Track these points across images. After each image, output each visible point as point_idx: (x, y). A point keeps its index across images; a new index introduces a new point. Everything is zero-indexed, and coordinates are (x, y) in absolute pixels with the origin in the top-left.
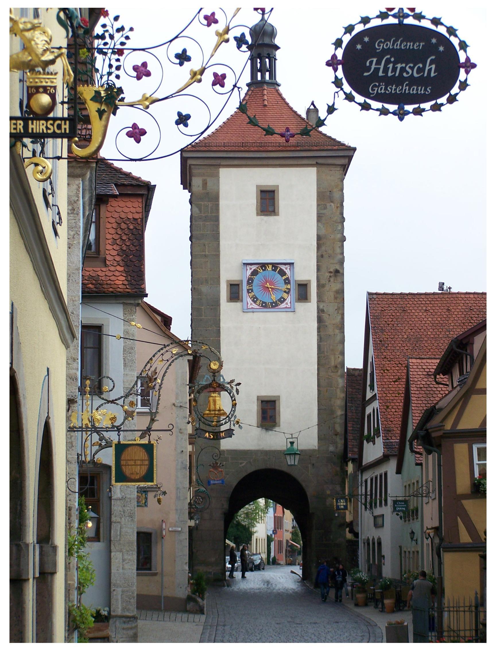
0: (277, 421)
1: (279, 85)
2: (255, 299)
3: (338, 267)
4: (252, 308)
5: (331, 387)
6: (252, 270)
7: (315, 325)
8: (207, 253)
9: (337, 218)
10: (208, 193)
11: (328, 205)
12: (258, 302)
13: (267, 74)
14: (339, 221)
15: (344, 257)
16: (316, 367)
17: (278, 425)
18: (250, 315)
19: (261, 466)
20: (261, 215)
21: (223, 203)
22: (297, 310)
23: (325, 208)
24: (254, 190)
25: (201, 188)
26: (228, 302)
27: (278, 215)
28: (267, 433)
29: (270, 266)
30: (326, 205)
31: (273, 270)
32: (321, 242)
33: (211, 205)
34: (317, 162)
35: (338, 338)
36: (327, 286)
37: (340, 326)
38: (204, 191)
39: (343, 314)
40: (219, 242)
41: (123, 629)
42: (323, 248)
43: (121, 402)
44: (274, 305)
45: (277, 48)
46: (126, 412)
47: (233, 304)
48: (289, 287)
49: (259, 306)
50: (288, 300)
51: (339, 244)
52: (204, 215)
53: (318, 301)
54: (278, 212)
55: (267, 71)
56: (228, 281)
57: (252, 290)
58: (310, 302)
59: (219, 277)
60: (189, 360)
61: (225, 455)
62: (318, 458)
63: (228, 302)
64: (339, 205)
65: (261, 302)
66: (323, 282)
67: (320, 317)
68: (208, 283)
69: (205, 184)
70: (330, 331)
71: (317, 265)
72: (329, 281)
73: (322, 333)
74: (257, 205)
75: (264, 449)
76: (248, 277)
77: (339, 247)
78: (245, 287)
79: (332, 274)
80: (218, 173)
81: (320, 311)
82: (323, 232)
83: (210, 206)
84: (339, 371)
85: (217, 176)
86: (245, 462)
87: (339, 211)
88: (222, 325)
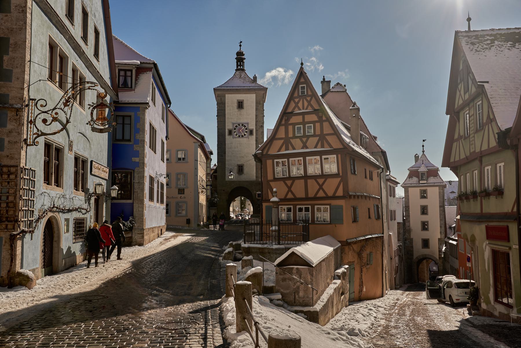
1: (245, 70)
3: (262, 125)
7: (255, 142)
9: (262, 109)
11: (259, 106)
13: (242, 67)
18: (235, 139)
23: (258, 107)
41: (138, 234)
43: (50, 112)
44: (242, 136)
45: (245, 59)
46: (53, 118)
55: (242, 66)
56: (228, 129)
60: (199, 145)
66: (257, 129)
69: (221, 99)
81: (256, 138)
85: (225, 97)
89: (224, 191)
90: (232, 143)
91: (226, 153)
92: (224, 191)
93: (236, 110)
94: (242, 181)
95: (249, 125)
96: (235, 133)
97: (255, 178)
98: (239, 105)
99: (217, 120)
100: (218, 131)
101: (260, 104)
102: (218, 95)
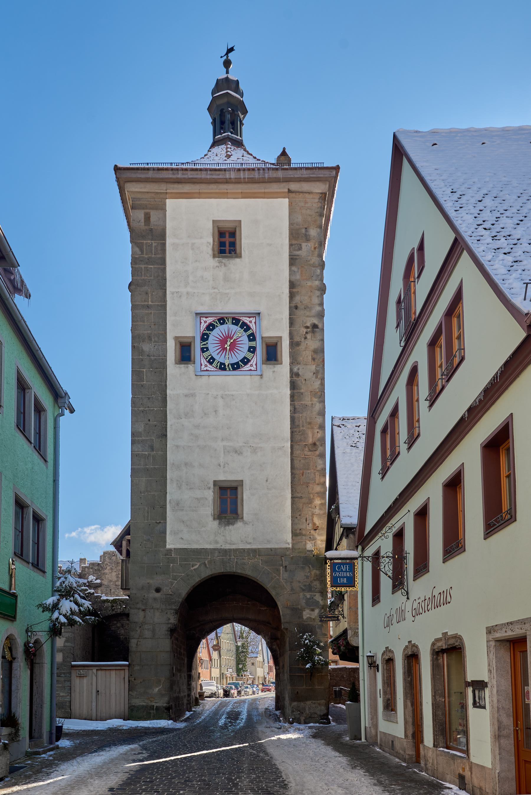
0: (239, 512)
2: (211, 360)
3: (316, 321)
4: (207, 370)
5: (308, 469)
6: (207, 324)
7: (288, 392)
8: (150, 303)
10: (151, 230)
11: (304, 245)
12: (214, 364)
14: (317, 263)
15: (323, 310)
16: (289, 444)
17: (240, 517)
18: (204, 379)
19: (218, 569)
20: (219, 257)
21: (169, 241)
22: (264, 376)
23: (300, 249)
24: (210, 225)
25: (143, 224)
26: (176, 363)
27: (240, 256)
28: (227, 528)
29: (230, 320)
30: (300, 245)
31: (233, 323)
32: (294, 290)
33: (156, 244)
34: (289, 191)
35: (318, 406)
36: (302, 344)
37: (319, 394)
38: (146, 227)
39: (323, 379)
40: (166, 289)
42: (297, 299)
44: (236, 367)
47: (182, 366)
48: (253, 344)
49: (216, 368)
50: (253, 362)
51: (318, 293)
52: (146, 256)
53: (292, 364)
54: (241, 254)
56: (176, 338)
57: (207, 349)
58: (281, 364)
59: (166, 333)
61: (173, 555)
62: (292, 558)
63: (176, 363)
64: (317, 245)
65: (219, 364)
66: (297, 339)
67: (294, 382)
68: (151, 340)
69: (147, 218)
70: (307, 400)
71: (290, 319)
72: (306, 338)
73: (296, 403)
74: (213, 245)
75: (222, 548)
76: (202, 332)
77: (318, 296)
78: (198, 345)
79: (309, 330)
80: (165, 204)
81: (294, 375)
82: (298, 277)
83: (154, 245)
84: (319, 449)
85: (163, 208)
86: (199, 564)
87: (316, 253)
88: (168, 392)
89: (158, 590)
90: (193, 395)
91: (170, 434)
92: (158, 590)
93: (212, 262)
94: (235, 550)
95: (265, 323)
96: (206, 354)
97: (288, 537)
98: (222, 244)
99: (132, 301)
100: (133, 347)
101: (307, 239)
102: (134, 199)
